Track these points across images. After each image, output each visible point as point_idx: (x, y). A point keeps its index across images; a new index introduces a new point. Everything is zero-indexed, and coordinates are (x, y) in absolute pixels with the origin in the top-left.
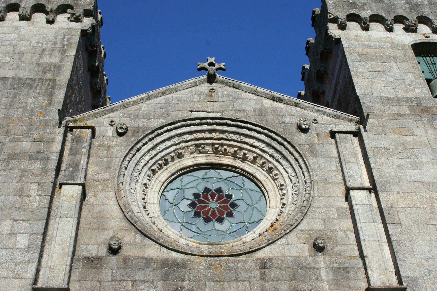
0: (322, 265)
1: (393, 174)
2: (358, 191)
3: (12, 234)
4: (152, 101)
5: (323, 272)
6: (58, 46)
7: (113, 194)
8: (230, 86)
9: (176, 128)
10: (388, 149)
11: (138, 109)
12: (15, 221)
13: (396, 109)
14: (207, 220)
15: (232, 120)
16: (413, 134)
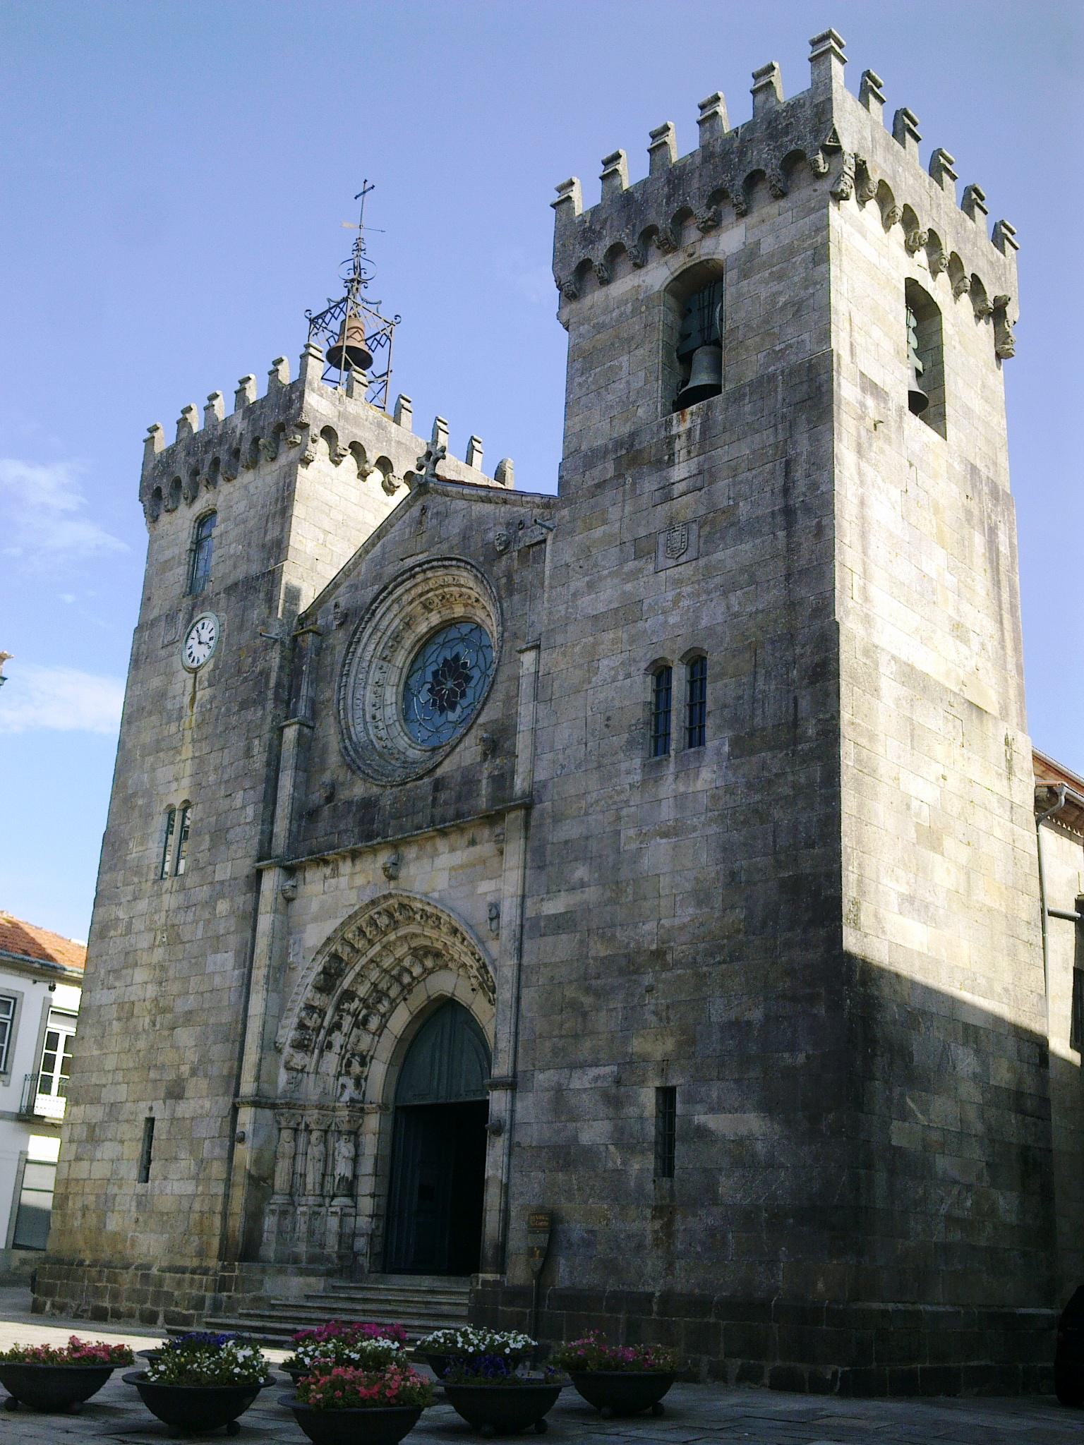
0: (486, 774)
1: (563, 613)
2: (528, 653)
3: (244, 807)
4: (370, 556)
5: (484, 782)
6: (279, 506)
7: (331, 719)
8: (439, 494)
9: (390, 593)
10: (567, 566)
11: (359, 573)
12: (245, 790)
13: (595, 475)
14: (442, 709)
15: (438, 560)
16: (605, 522)
